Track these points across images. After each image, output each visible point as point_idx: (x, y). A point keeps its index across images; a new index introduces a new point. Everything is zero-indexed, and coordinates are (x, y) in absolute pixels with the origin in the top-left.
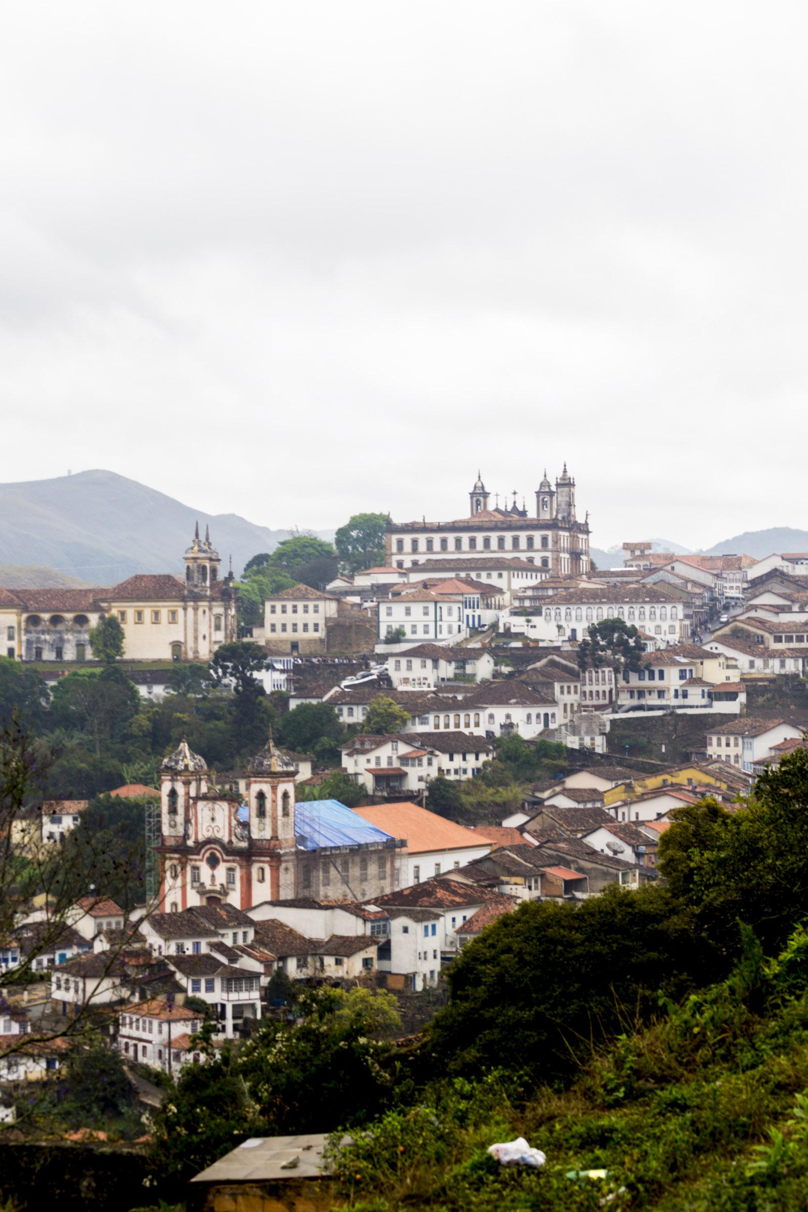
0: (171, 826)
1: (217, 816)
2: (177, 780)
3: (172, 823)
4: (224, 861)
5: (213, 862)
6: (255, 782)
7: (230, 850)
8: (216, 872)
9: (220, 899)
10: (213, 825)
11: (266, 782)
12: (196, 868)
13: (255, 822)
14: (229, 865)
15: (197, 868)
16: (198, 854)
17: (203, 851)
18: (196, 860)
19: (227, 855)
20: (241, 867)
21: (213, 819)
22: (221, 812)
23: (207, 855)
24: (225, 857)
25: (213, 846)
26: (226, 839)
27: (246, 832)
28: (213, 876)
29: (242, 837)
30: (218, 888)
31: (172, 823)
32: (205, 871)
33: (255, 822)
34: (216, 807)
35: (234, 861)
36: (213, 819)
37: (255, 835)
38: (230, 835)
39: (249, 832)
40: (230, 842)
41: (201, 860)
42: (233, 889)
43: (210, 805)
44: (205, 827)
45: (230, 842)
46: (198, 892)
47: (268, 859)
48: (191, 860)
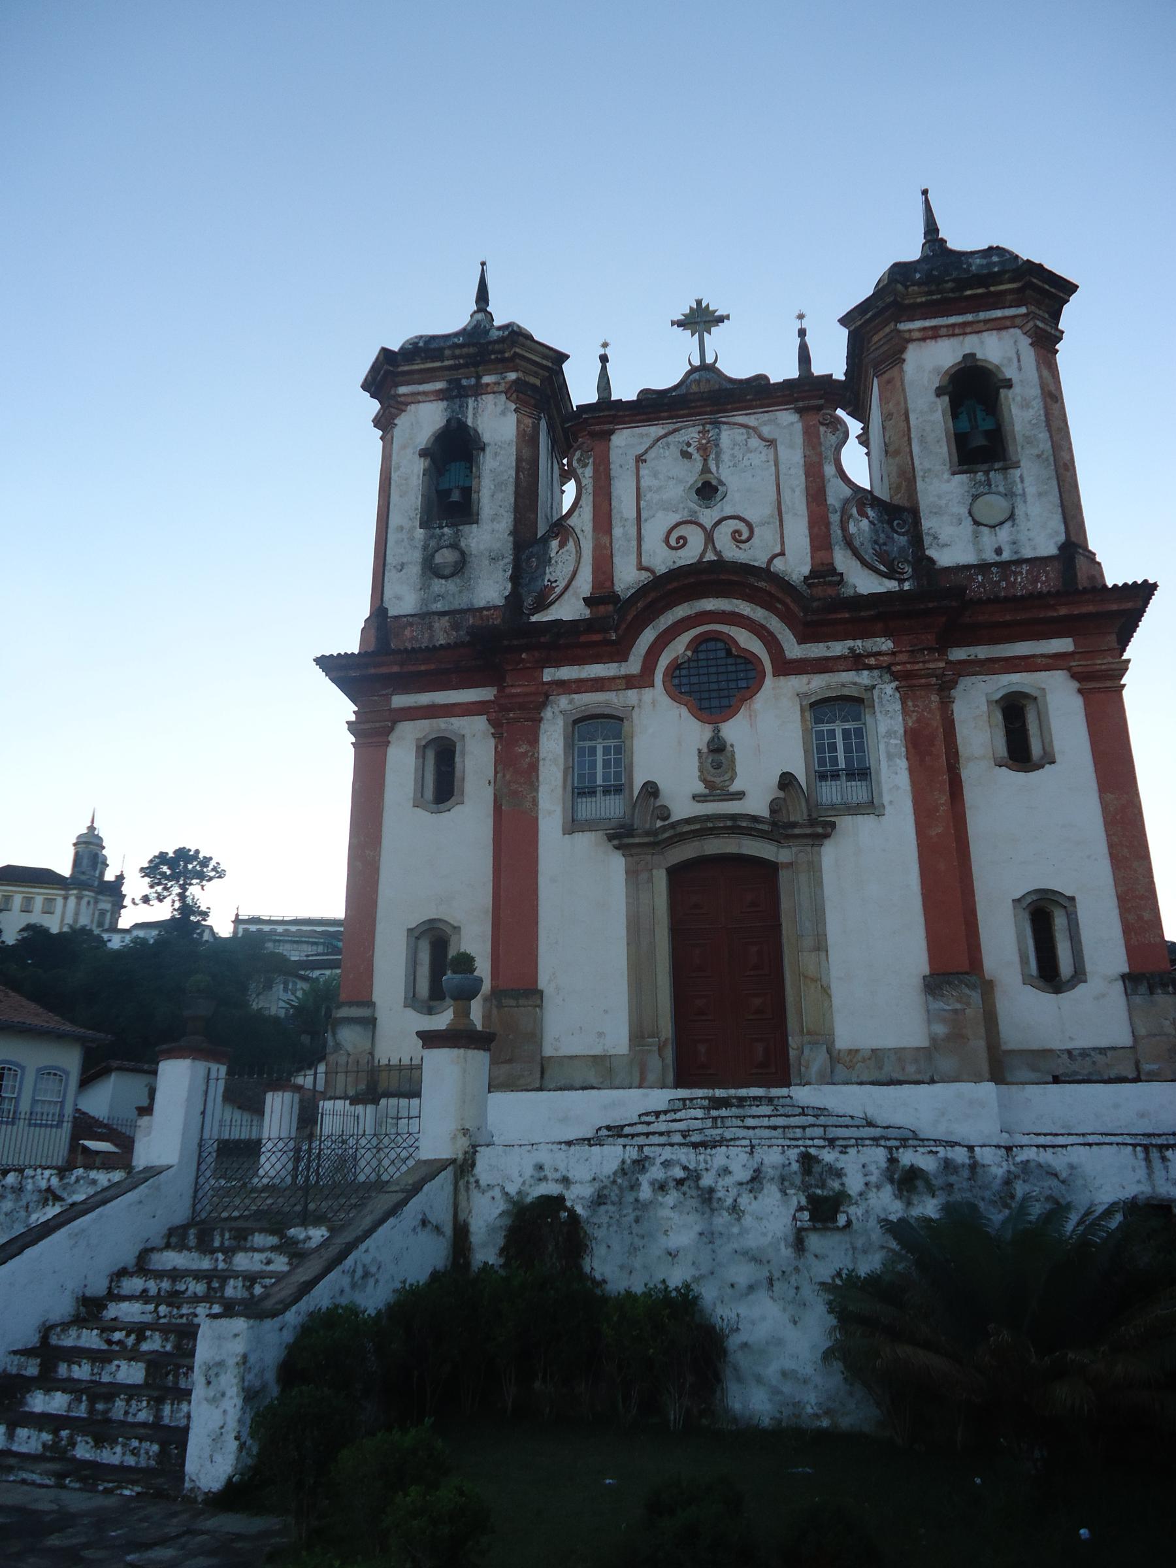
0: (431, 569)
1: (725, 473)
2: (479, 390)
3: (445, 557)
4: (786, 667)
5: (716, 684)
6: (933, 334)
7: (819, 608)
8: (734, 730)
9: (768, 870)
10: (708, 517)
11: (999, 326)
12: (602, 729)
13: (943, 493)
14: (817, 684)
15: (612, 724)
16: (619, 653)
17: (648, 636)
18: (598, 684)
19: (802, 639)
20: (908, 683)
21: (707, 491)
22: (760, 457)
23: (679, 647)
24: (794, 650)
25: (710, 604)
26: (796, 564)
27: (902, 540)
28: (717, 754)
29: (882, 556)
30: (757, 804)
31: (445, 557)
32: (664, 743)
33: (943, 493)
34: (727, 437)
35: (857, 662)
36: (707, 491)
37: (953, 545)
38: (820, 541)
39: (917, 539)
40: (824, 573)
41: (642, 680)
42: (872, 807)
43: (691, 434)
44: (655, 531)
45: (824, 573)
46: (610, 838)
47: (1063, 645)
48: (565, 686)
